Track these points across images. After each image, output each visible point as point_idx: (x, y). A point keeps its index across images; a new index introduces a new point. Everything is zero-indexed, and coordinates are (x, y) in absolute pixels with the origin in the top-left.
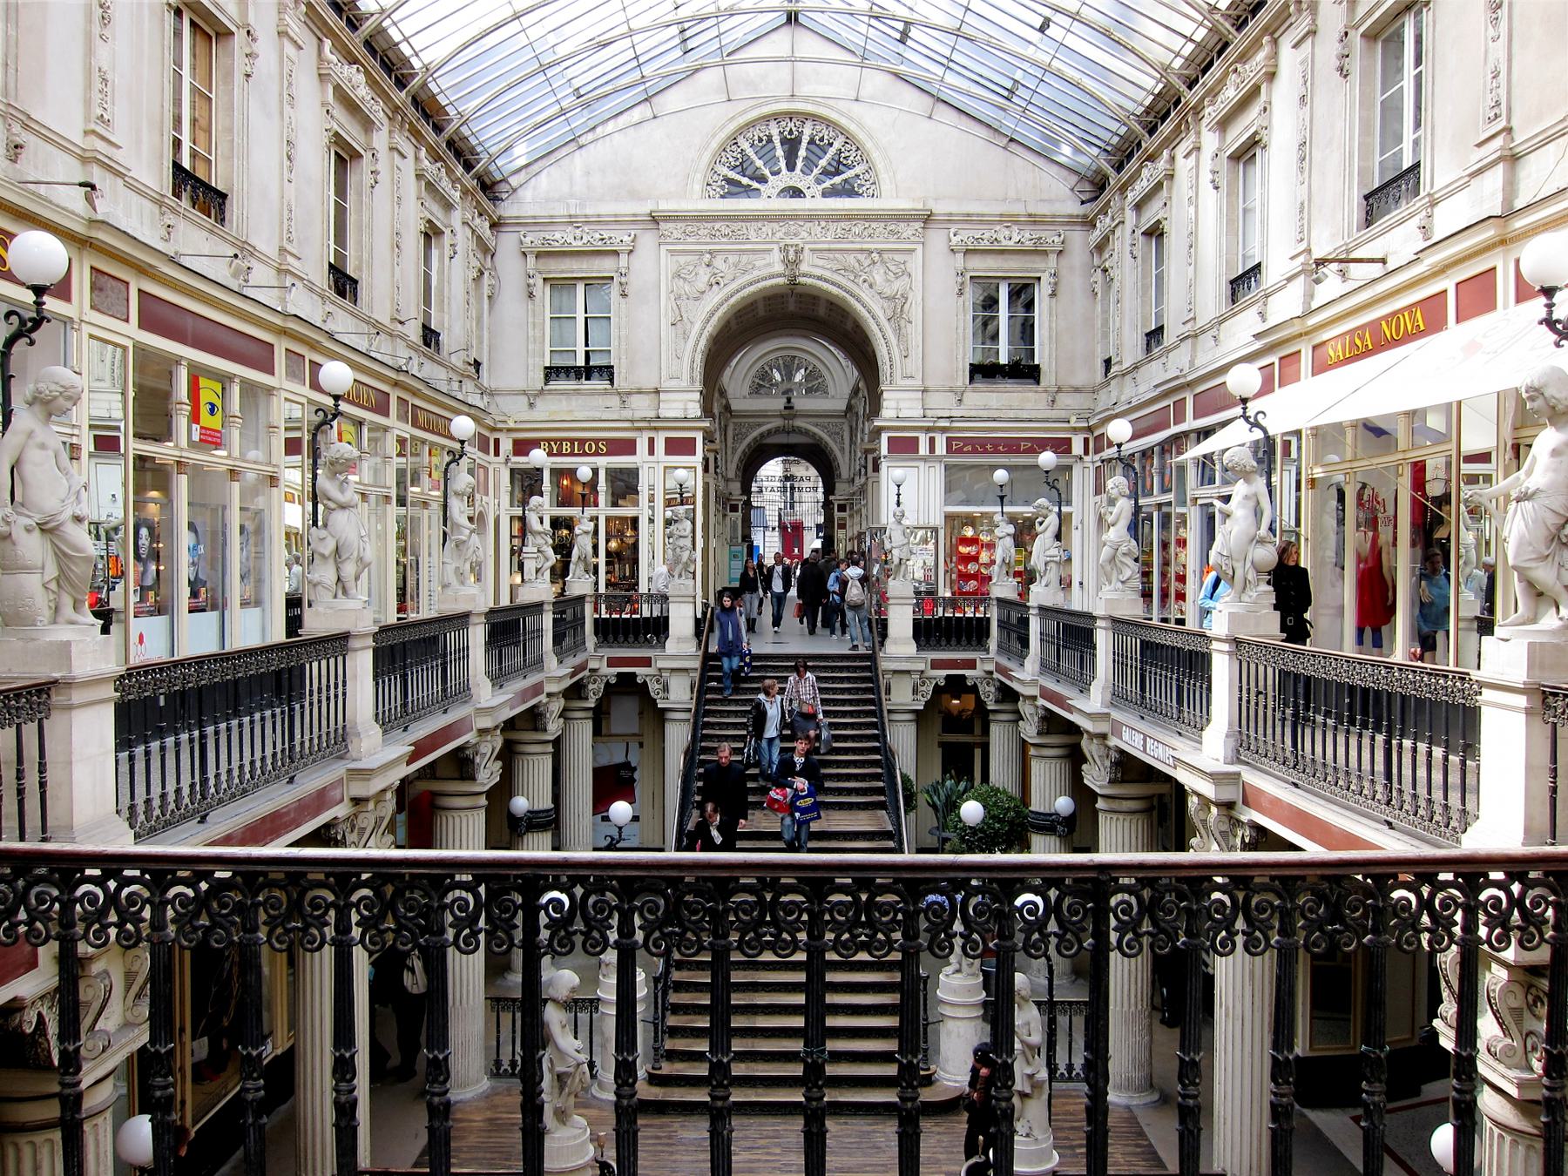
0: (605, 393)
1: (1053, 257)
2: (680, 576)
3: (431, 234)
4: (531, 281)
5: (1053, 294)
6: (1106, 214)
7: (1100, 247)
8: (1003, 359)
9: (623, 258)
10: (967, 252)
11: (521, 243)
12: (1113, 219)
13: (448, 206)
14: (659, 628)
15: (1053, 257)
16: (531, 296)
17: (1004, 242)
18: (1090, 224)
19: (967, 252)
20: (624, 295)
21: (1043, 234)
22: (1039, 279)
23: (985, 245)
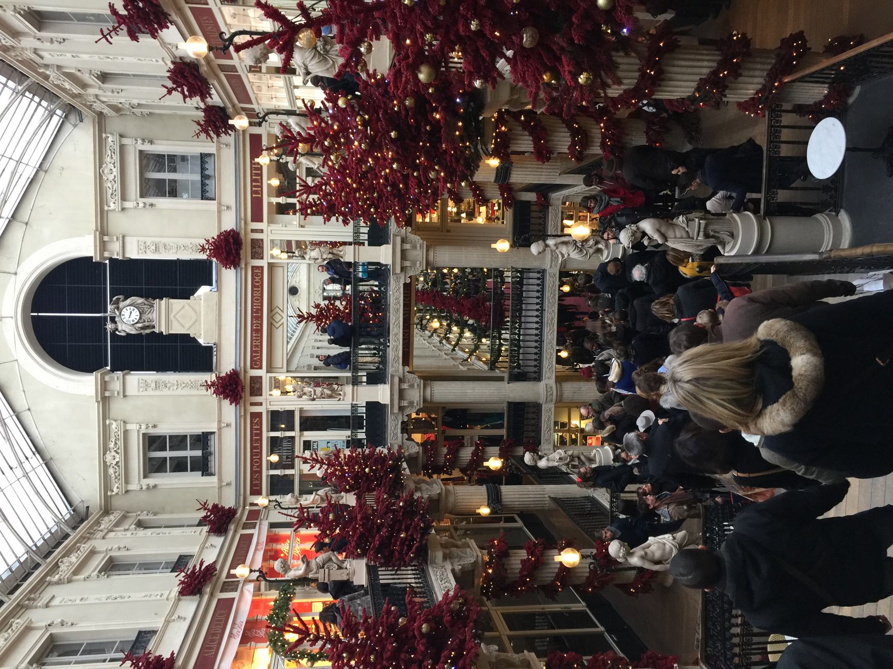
0: (220, 436)
1: (125, 141)
2: (340, 394)
3: (112, 566)
4: (144, 487)
5: (151, 142)
6: (91, 105)
7: (116, 109)
8: (197, 177)
9: (129, 427)
10: (124, 198)
11: (117, 494)
12: (95, 102)
13: (93, 553)
14: (374, 407)
15: (125, 141)
16: (155, 486)
17: (115, 173)
18: (101, 115)
19: (124, 198)
20: (155, 426)
21: (108, 148)
22: (141, 152)
23: (117, 186)
